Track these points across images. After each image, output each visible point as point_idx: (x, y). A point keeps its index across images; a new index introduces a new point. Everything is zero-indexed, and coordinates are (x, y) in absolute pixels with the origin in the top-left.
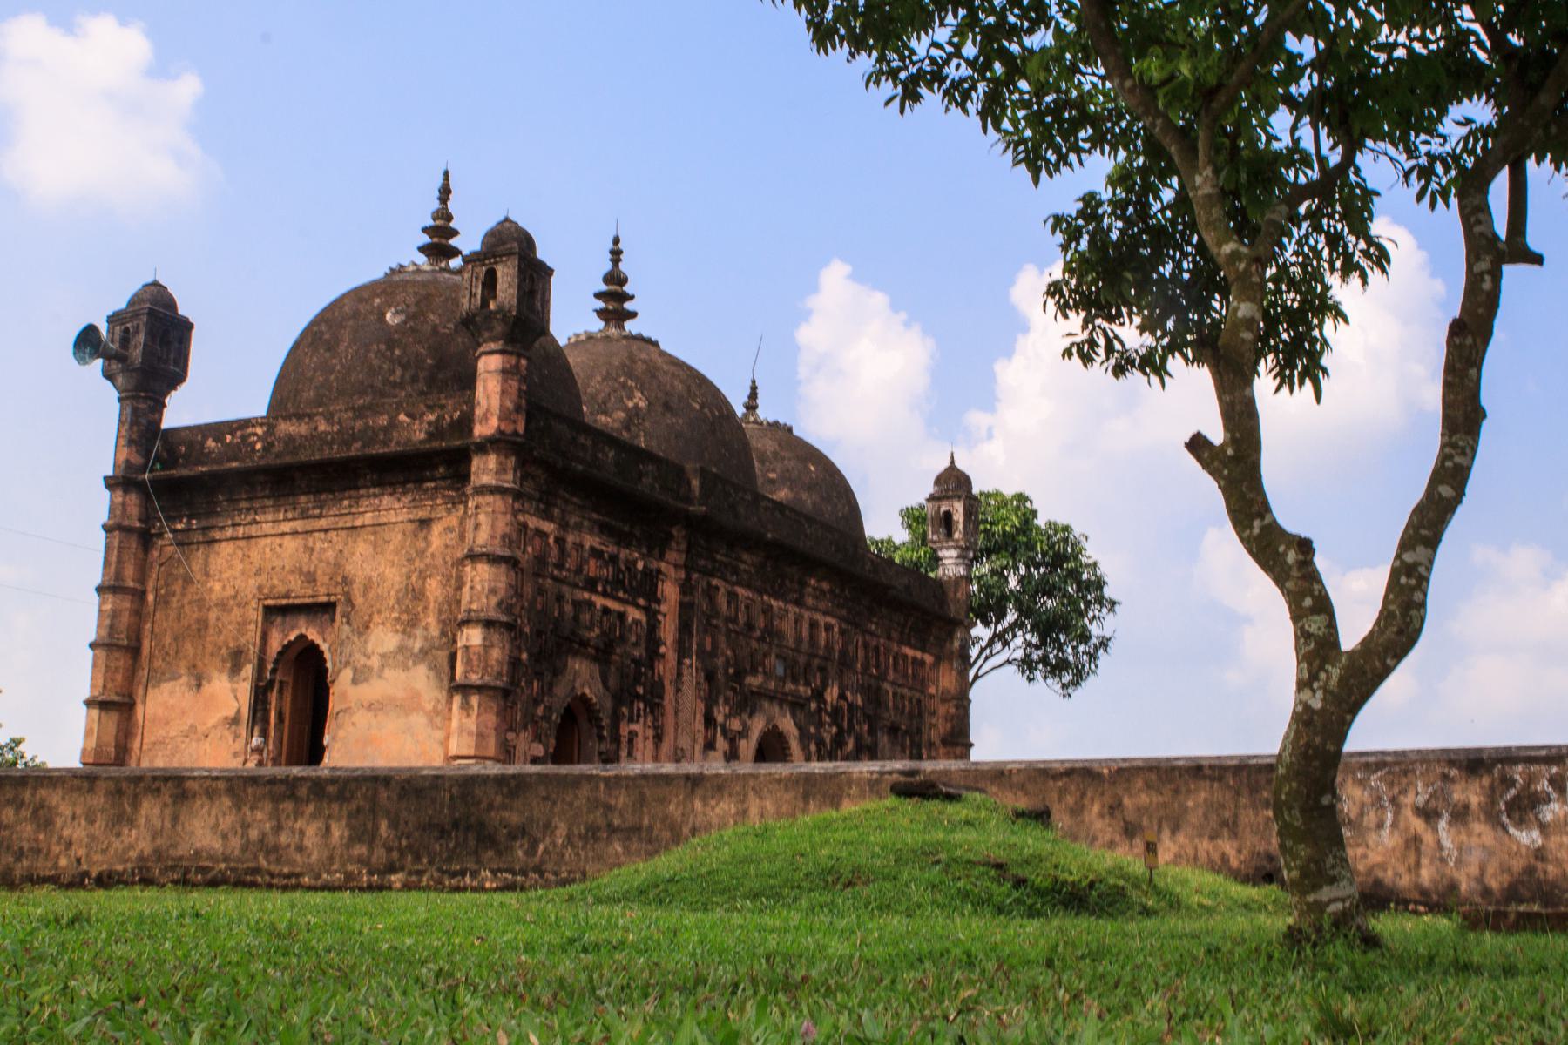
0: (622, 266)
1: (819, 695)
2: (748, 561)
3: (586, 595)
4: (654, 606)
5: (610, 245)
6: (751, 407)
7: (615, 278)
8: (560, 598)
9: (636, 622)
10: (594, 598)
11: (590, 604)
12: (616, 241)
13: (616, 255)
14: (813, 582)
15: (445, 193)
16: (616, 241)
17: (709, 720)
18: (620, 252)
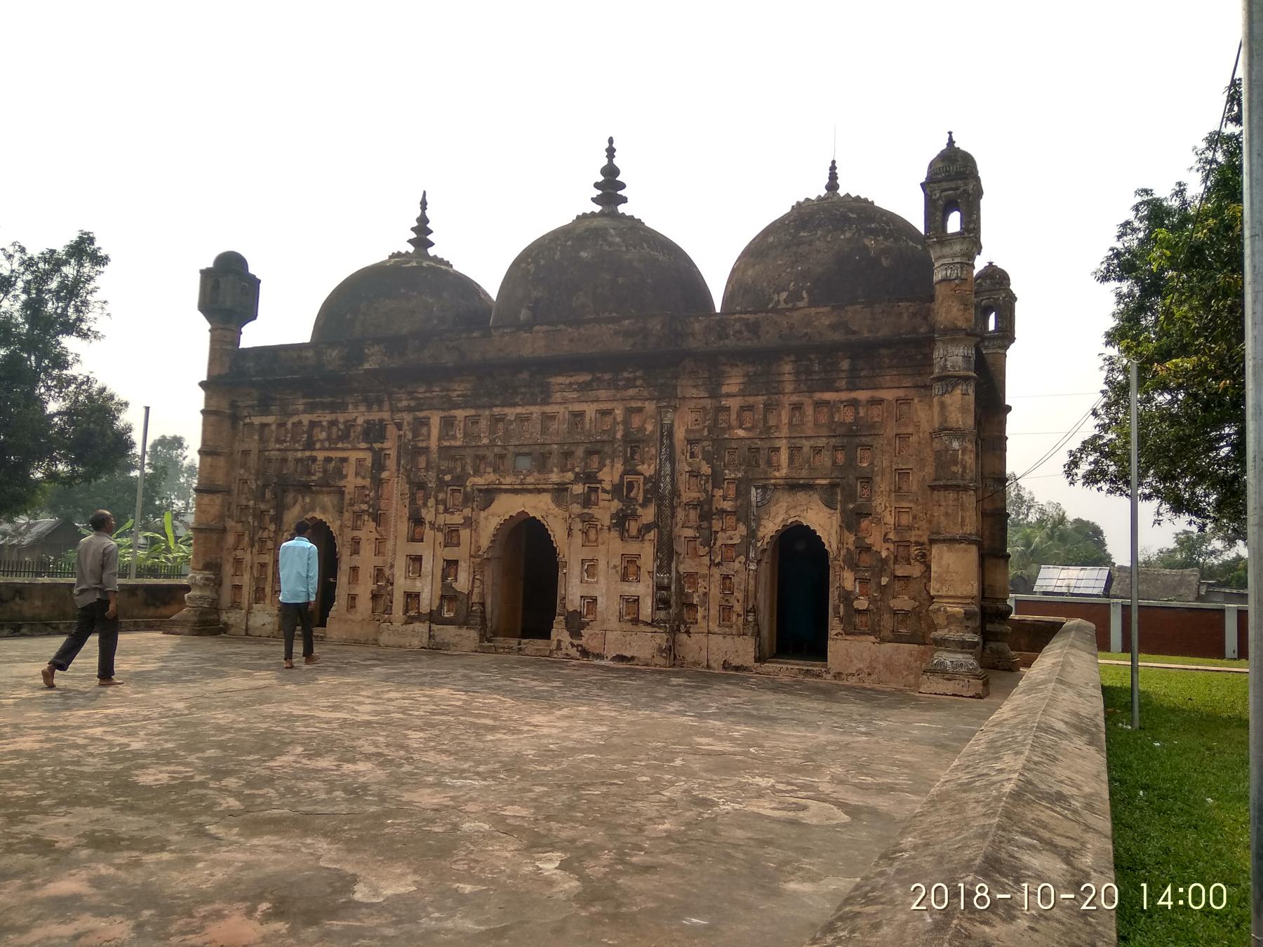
0: (615, 161)
1: (589, 478)
2: (459, 389)
3: (308, 453)
4: (377, 446)
5: (607, 145)
6: (833, 185)
7: (610, 172)
8: (284, 460)
9: (360, 462)
10: (314, 453)
11: (314, 459)
12: (611, 141)
13: (611, 152)
14: (560, 379)
15: (424, 204)
16: (611, 141)
17: (417, 520)
18: (615, 150)
